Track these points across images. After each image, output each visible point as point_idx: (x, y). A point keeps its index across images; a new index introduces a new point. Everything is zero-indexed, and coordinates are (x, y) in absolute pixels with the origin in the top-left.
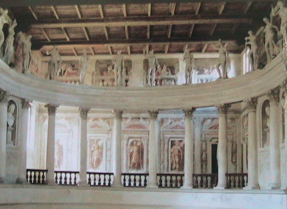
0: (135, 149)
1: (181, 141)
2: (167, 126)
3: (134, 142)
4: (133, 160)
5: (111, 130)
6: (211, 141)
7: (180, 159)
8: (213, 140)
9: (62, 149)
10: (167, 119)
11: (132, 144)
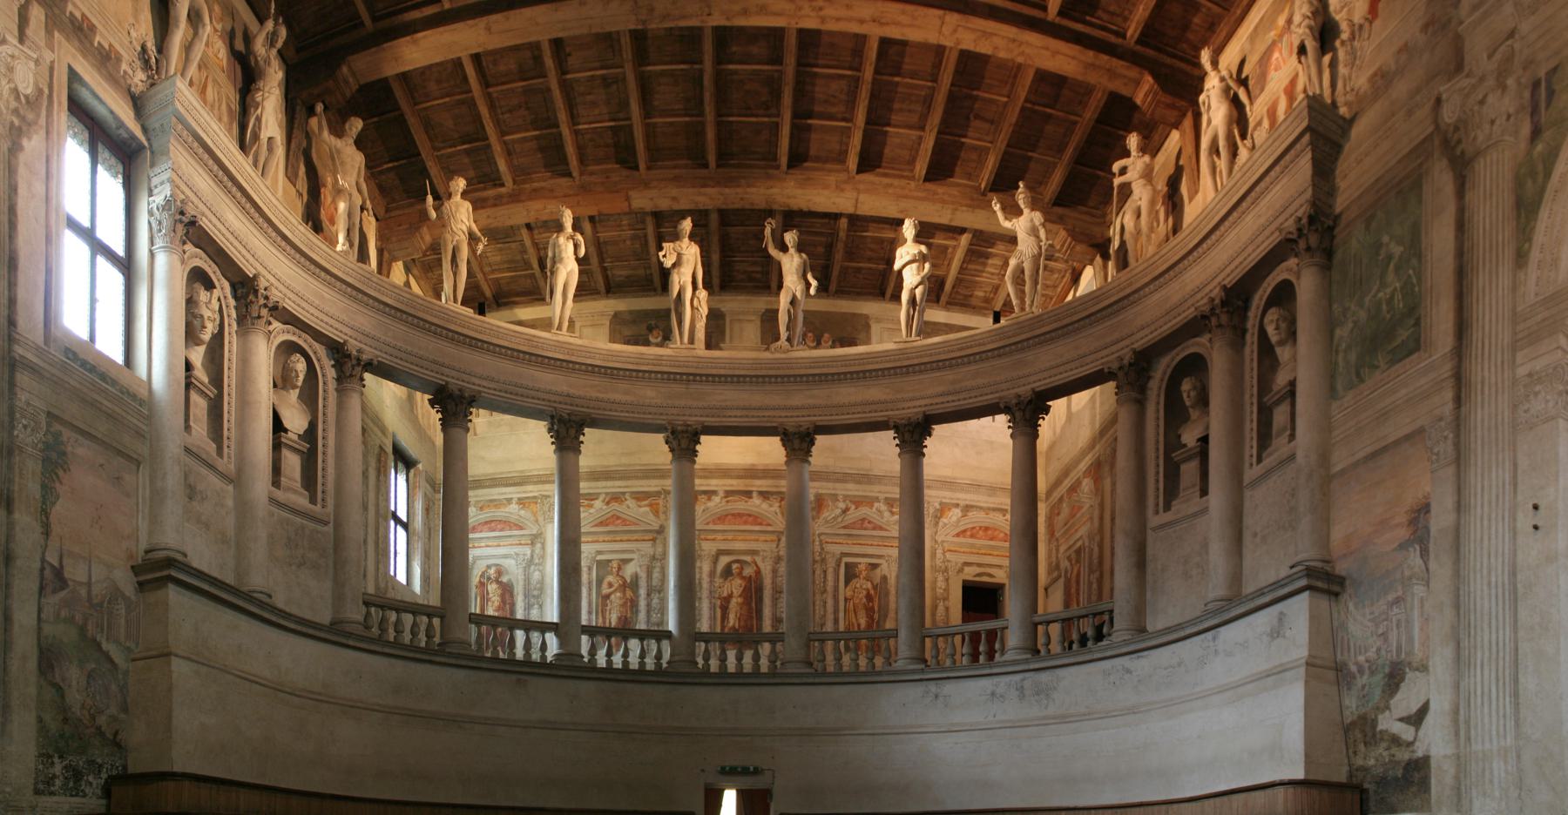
0: (736, 586)
1: (874, 566)
2: (835, 518)
3: (734, 566)
4: (732, 620)
5: (661, 530)
6: (961, 571)
7: (870, 617)
8: (967, 569)
9: (512, 595)
10: (835, 497)
11: (727, 572)
